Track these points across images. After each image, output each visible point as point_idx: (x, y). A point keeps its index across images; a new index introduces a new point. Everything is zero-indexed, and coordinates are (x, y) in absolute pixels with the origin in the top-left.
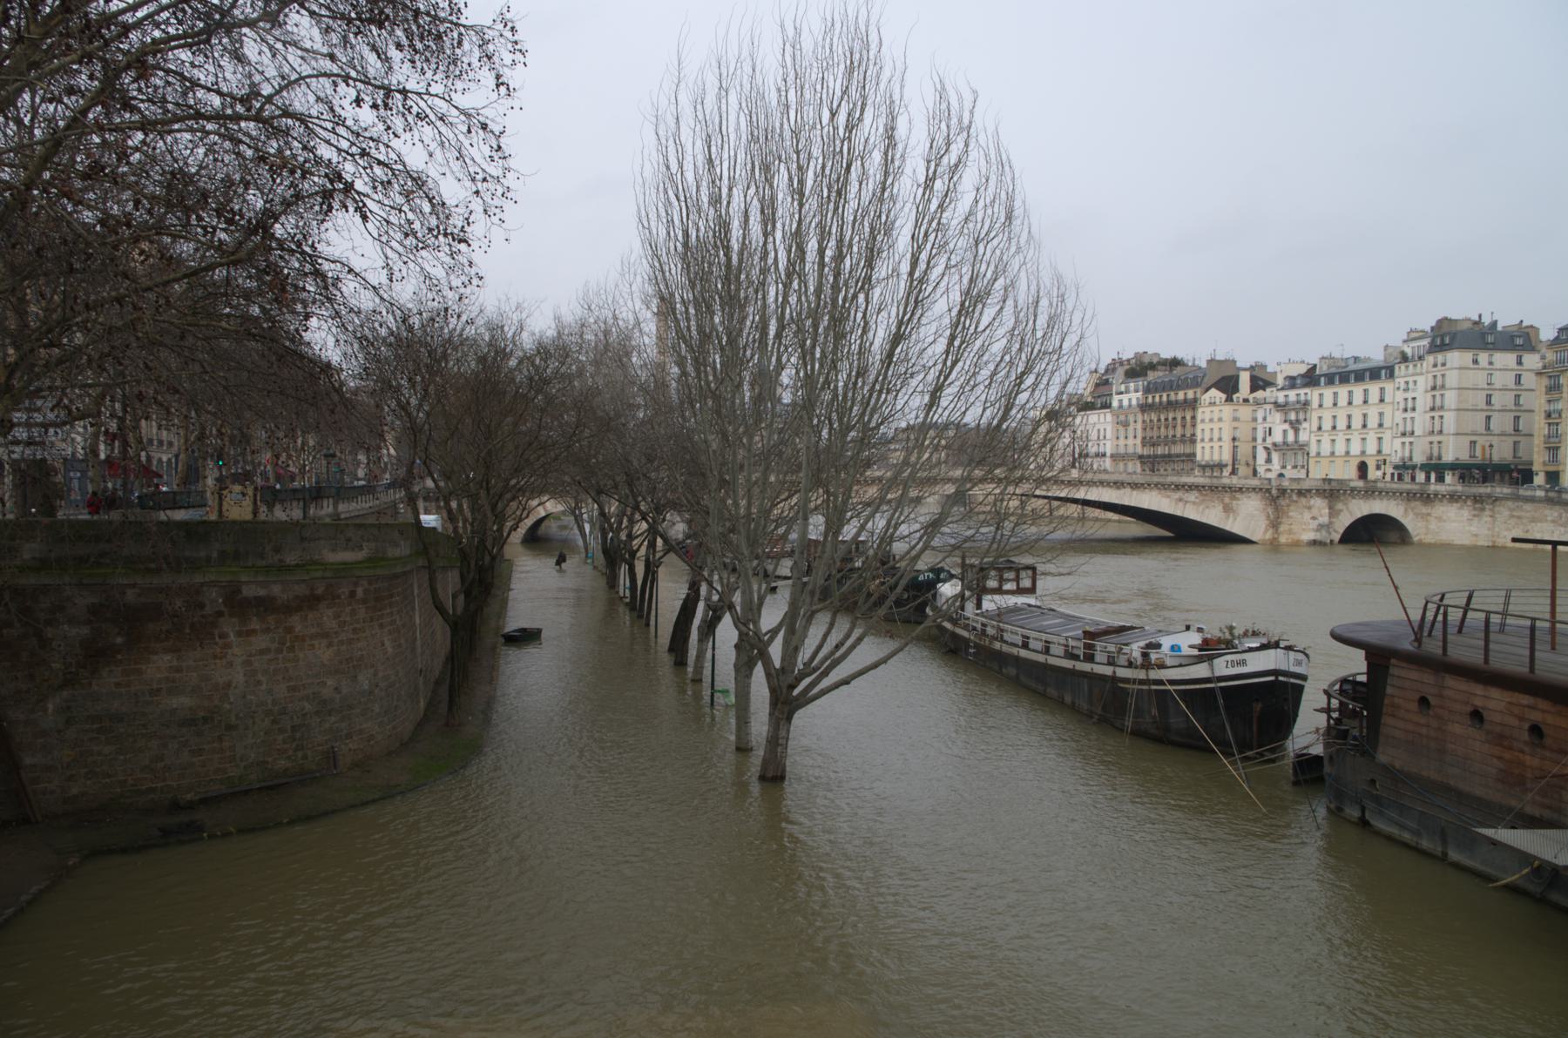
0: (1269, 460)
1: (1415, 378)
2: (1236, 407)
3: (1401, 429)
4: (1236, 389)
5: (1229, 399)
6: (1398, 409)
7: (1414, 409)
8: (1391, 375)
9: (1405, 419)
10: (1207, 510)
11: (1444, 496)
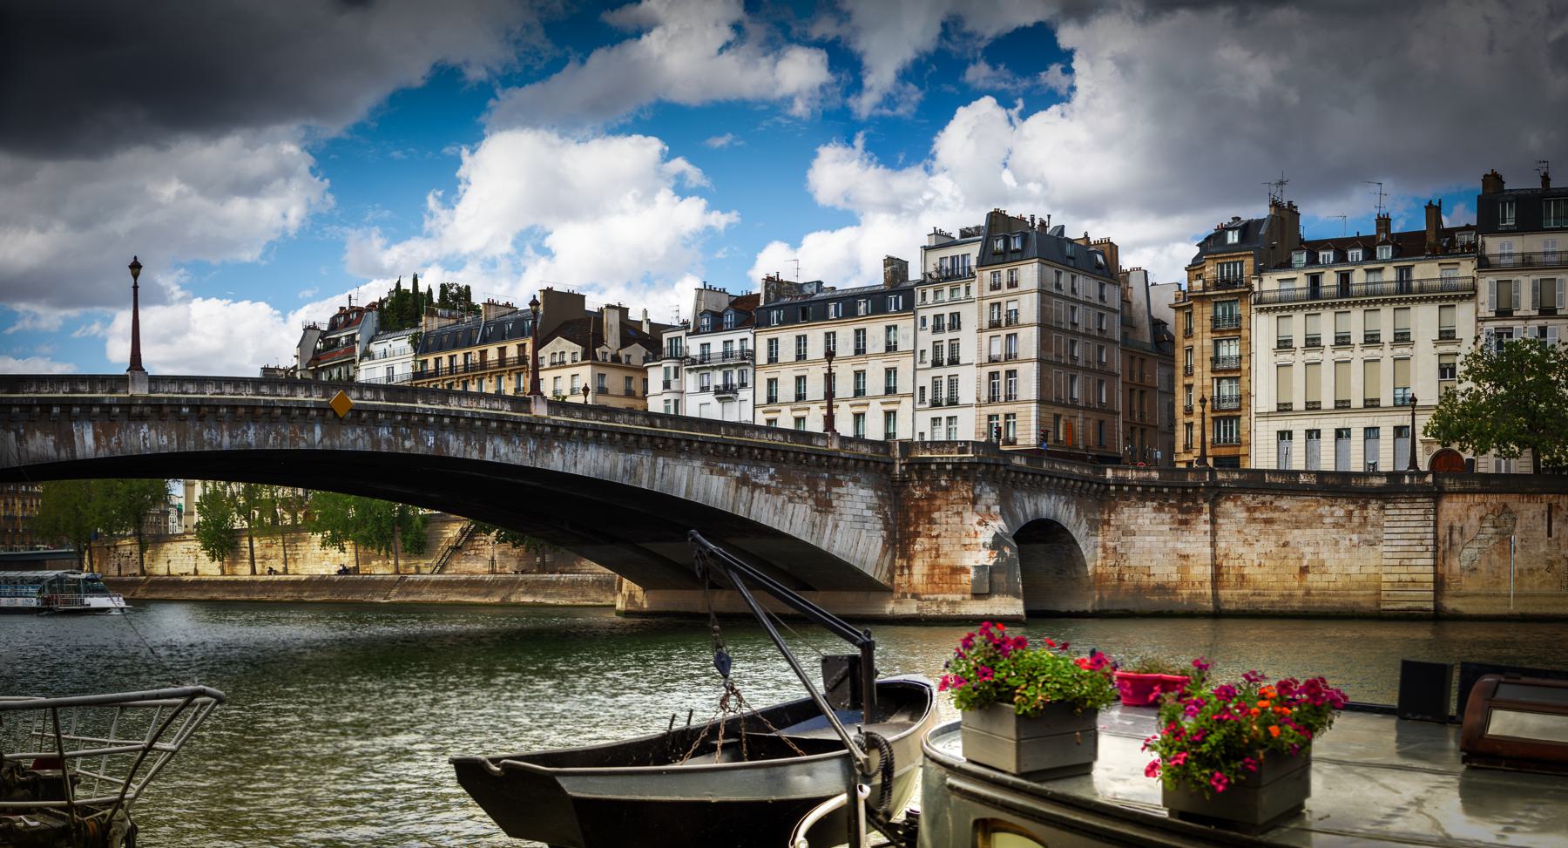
2: (602, 371)
3: (928, 396)
4: (599, 340)
5: (590, 356)
7: (954, 361)
8: (909, 307)
10: (791, 506)
11: (1133, 487)
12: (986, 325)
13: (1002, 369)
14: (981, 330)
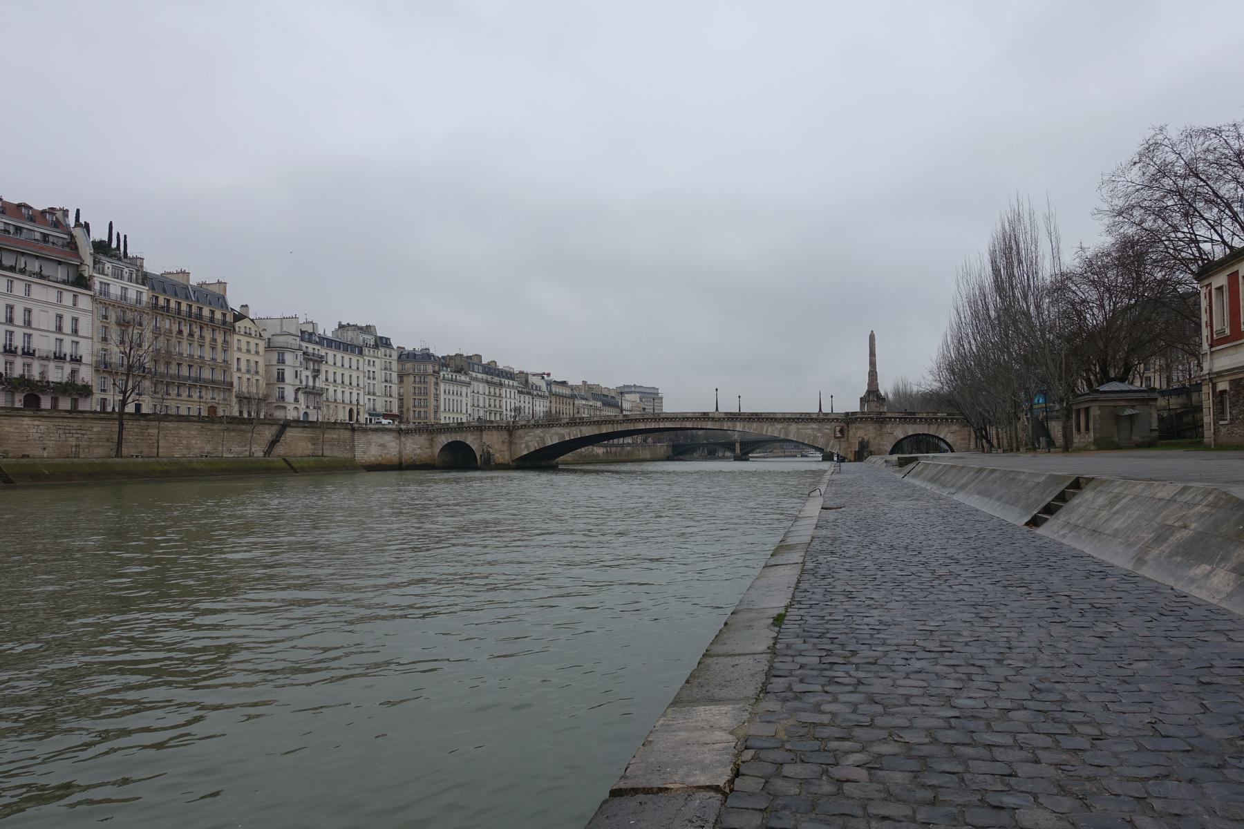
0: (296, 400)
1: (374, 359)
7: (374, 379)
9: (369, 383)
13: (388, 385)
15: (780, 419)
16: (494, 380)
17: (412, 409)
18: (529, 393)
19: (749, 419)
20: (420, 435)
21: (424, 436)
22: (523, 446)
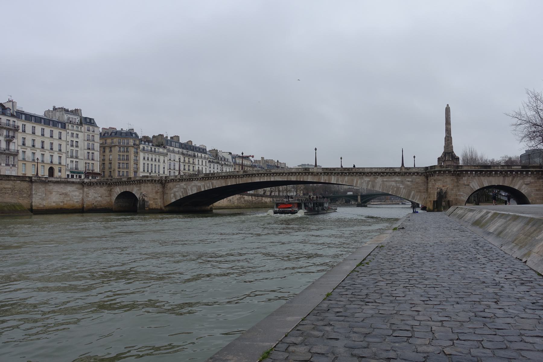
1: (77, 133)
3: (69, 154)
6: (68, 145)
7: (77, 146)
12: (86, 139)
13: (91, 152)
14: (84, 140)
15: (368, 173)
16: (189, 153)
17: (117, 170)
18: (218, 163)
19: (342, 173)
20: (101, 187)
21: (104, 188)
22: (173, 195)
